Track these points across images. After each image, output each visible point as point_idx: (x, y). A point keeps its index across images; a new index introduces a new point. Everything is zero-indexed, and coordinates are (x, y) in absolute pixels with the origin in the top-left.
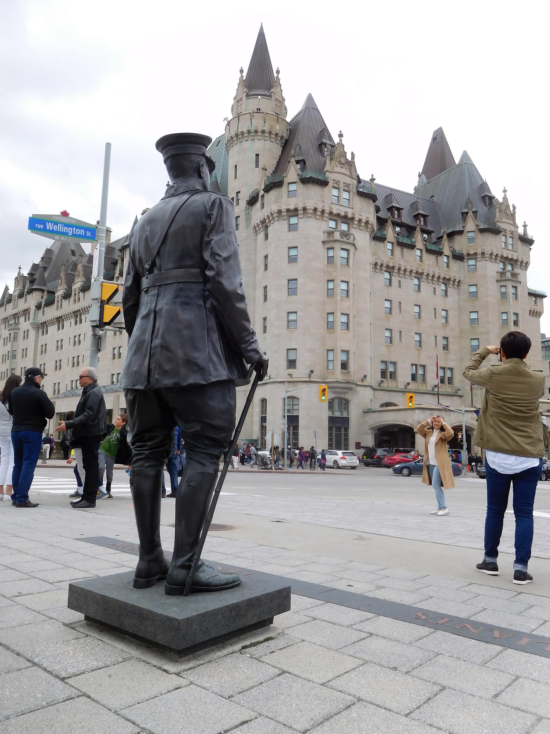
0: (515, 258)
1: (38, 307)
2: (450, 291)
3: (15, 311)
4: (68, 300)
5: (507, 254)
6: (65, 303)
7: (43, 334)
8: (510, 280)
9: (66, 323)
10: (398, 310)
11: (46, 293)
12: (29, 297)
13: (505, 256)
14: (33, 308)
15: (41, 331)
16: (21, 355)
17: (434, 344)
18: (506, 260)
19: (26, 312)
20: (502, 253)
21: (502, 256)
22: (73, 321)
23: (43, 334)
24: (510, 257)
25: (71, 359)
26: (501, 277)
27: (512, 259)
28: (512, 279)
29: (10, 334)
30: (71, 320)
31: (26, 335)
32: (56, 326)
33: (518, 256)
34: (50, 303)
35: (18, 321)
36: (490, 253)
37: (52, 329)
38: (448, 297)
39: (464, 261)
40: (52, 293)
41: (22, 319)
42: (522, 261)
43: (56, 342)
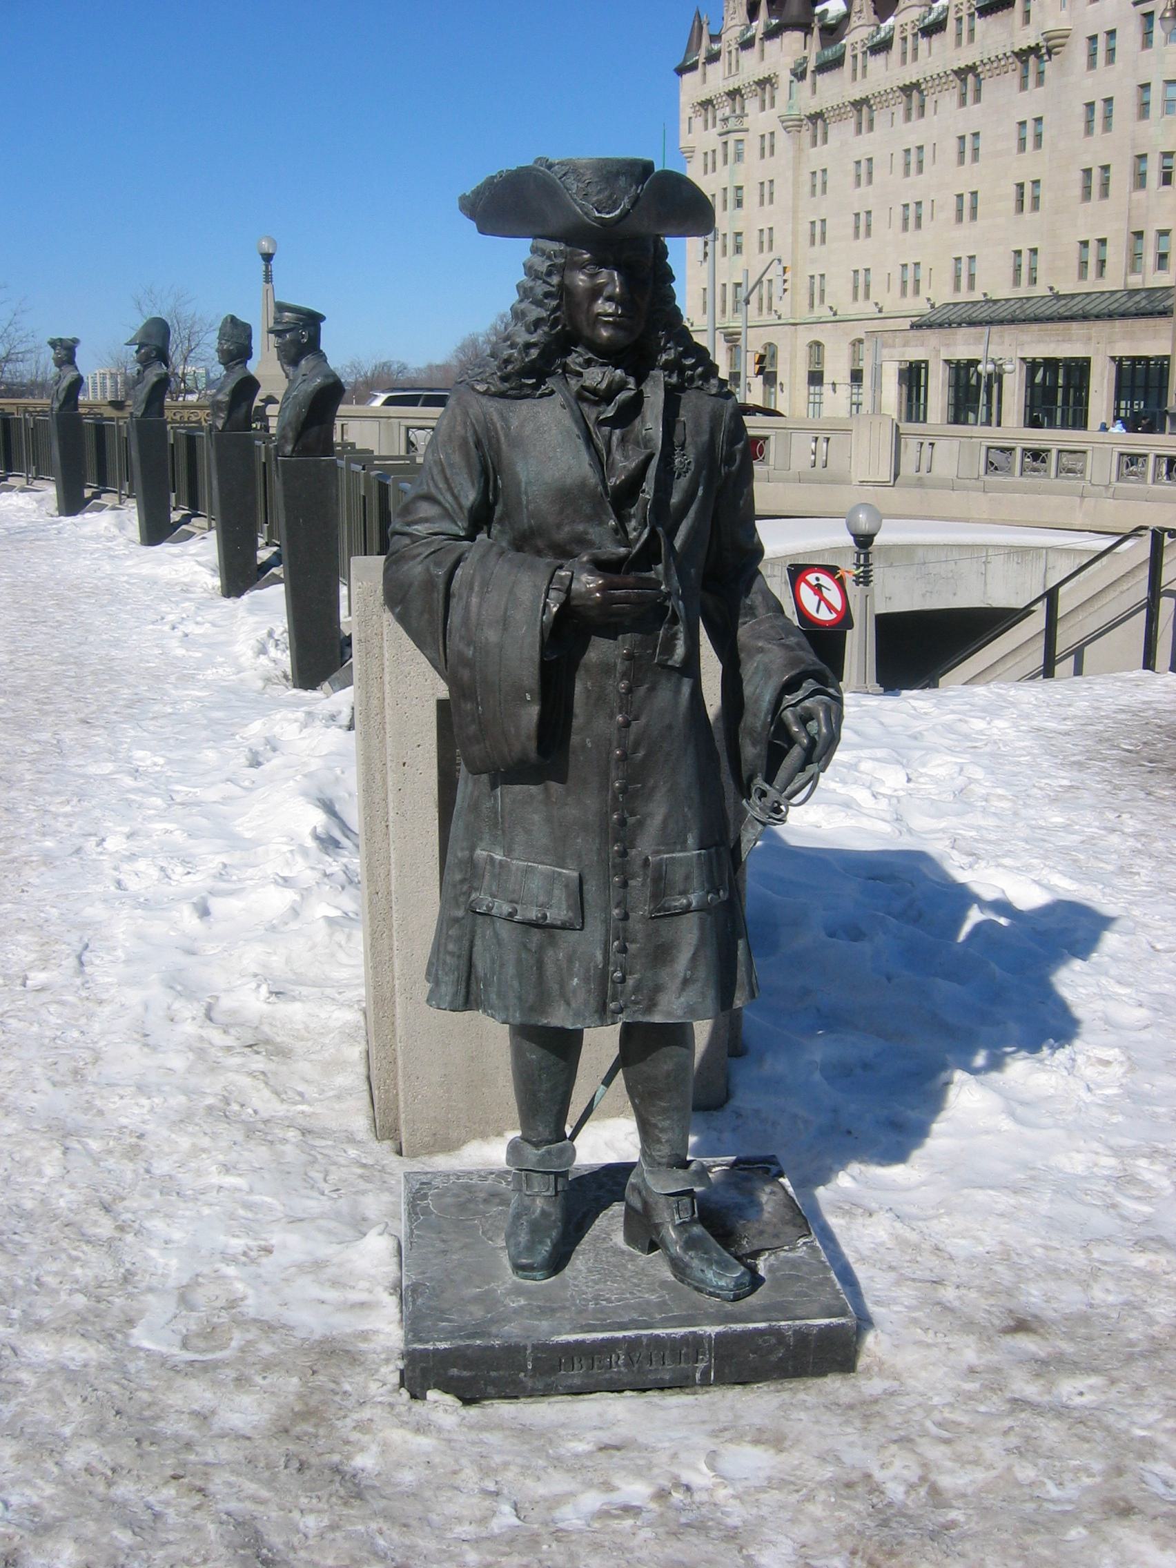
1: (799, 74)
3: (732, 84)
4: (882, 56)
6: (876, 63)
7: (814, 144)
9: (880, 118)
11: (816, 32)
12: (772, 46)
14: (785, 77)
15: (806, 135)
16: (757, 199)
19: (765, 83)
22: (900, 111)
23: (814, 144)
25: (899, 210)
29: (726, 143)
30: (894, 109)
31: (767, 146)
32: (852, 122)
34: (830, 65)
35: (743, 108)
37: (841, 132)
40: (833, 32)
41: (752, 105)
43: (852, 166)
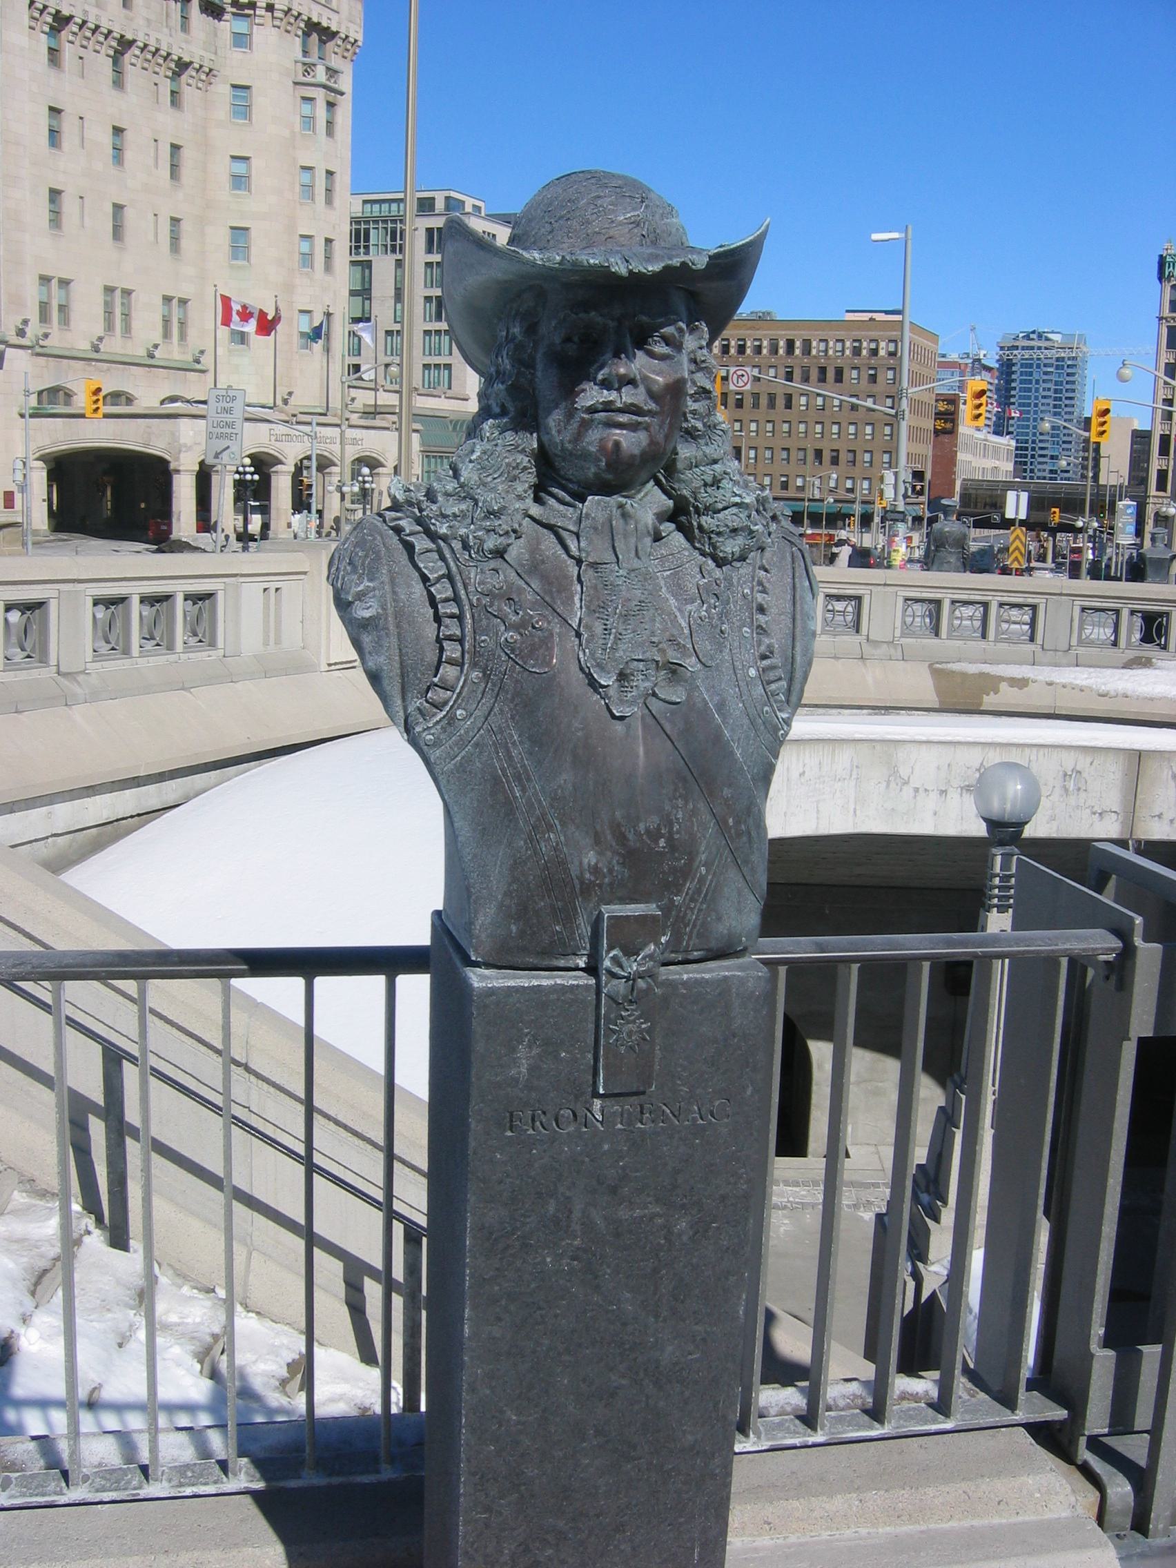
0: (334, 29)
2: (189, 94)
5: (320, 15)
8: (325, 87)
10: (77, 141)
13: (315, 20)
17: (151, 237)
18: (313, 27)
20: (310, 10)
21: (309, 19)
24: (325, 24)
26: (304, 75)
27: (328, 28)
28: (328, 83)
33: (339, 23)
36: (286, 9)
38: (183, 111)
39: (226, 17)
42: (347, 37)
